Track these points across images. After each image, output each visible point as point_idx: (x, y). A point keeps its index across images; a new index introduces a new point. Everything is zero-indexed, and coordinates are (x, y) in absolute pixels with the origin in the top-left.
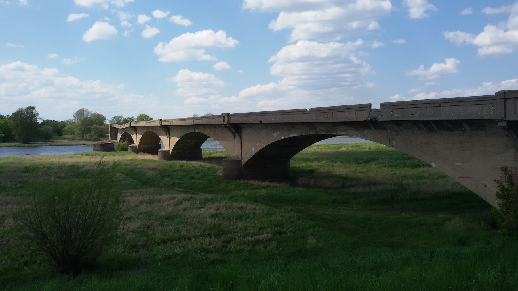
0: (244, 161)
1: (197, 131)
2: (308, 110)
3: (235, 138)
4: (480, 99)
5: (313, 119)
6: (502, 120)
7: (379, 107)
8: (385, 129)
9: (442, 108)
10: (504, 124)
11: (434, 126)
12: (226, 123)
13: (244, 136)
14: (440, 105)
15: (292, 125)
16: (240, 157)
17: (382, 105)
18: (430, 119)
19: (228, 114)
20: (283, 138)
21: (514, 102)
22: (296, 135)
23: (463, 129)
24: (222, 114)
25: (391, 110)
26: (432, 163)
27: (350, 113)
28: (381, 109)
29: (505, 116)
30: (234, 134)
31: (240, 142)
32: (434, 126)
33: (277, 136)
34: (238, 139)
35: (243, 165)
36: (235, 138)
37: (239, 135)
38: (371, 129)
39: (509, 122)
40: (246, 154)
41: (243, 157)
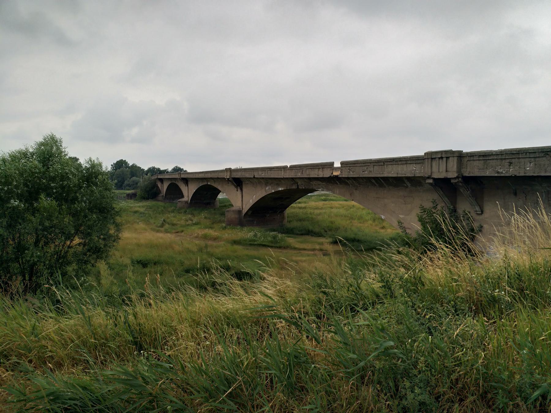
0: (245, 211)
1: (209, 184)
2: (289, 167)
3: (237, 191)
4: (412, 159)
5: (291, 175)
6: (429, 178)
7: (340, 166)
8: (347, 184)
9: (386, 166)
10: (431, 181)
11: (383, 182)
12: (228, 177)
13: (244, 190)
14: (384, 163)
15: (277, 181)
16: (241, 207)
17: (342, 163)
18: (379, 176)
19: (230, 169)
20: (273, 191)
21: (438, 162)
22: (283, 189)
23: (406, 185)
24: (226, 169)
25: (348, 168)
26: (382, 215)
27: (415, 175)
28: (341, 167)
29: (431, 174)
30: (236, 187)
31: (241, 195)
32: (383, 182)
33: (270, 190)
34: (239, 192)
35: (243, 215)
36: (237, 191)
37: (240, 187)
38: (385, 187)
39: (434, 179)
40: (246, 205)
41: (244, 208)
